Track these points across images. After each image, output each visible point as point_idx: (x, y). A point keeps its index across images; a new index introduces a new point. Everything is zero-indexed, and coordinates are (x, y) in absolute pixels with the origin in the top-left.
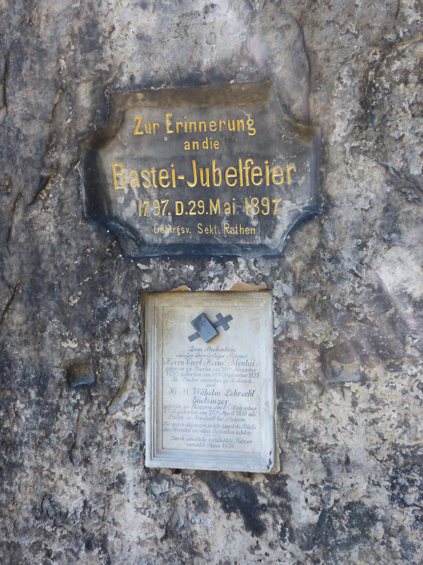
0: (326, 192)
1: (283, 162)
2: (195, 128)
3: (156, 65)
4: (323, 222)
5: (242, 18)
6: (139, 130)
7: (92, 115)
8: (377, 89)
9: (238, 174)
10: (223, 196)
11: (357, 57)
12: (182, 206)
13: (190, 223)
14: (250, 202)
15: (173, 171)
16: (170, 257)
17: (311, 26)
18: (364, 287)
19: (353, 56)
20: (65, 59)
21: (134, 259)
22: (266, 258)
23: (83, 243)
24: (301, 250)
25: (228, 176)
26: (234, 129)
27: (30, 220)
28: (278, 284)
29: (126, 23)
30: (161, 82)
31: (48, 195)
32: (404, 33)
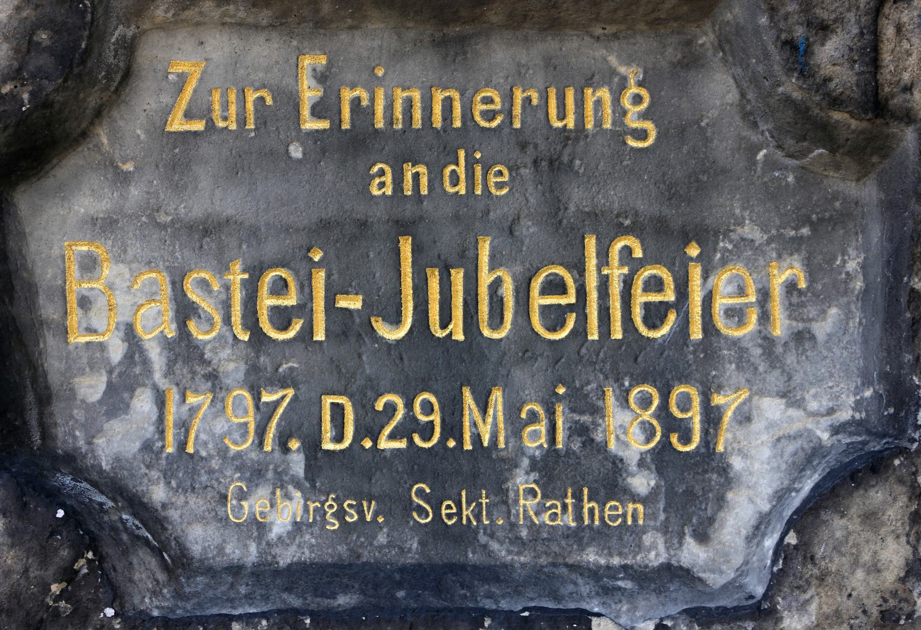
1: (759, 250)
2: (417, 114)
6: (189, 115)
7: (17, 50)
9: (582, 293)
13: (381, 483)
14: (624, 401)
15: (319, 279)
24: (841, 588)
25: (538, 301)
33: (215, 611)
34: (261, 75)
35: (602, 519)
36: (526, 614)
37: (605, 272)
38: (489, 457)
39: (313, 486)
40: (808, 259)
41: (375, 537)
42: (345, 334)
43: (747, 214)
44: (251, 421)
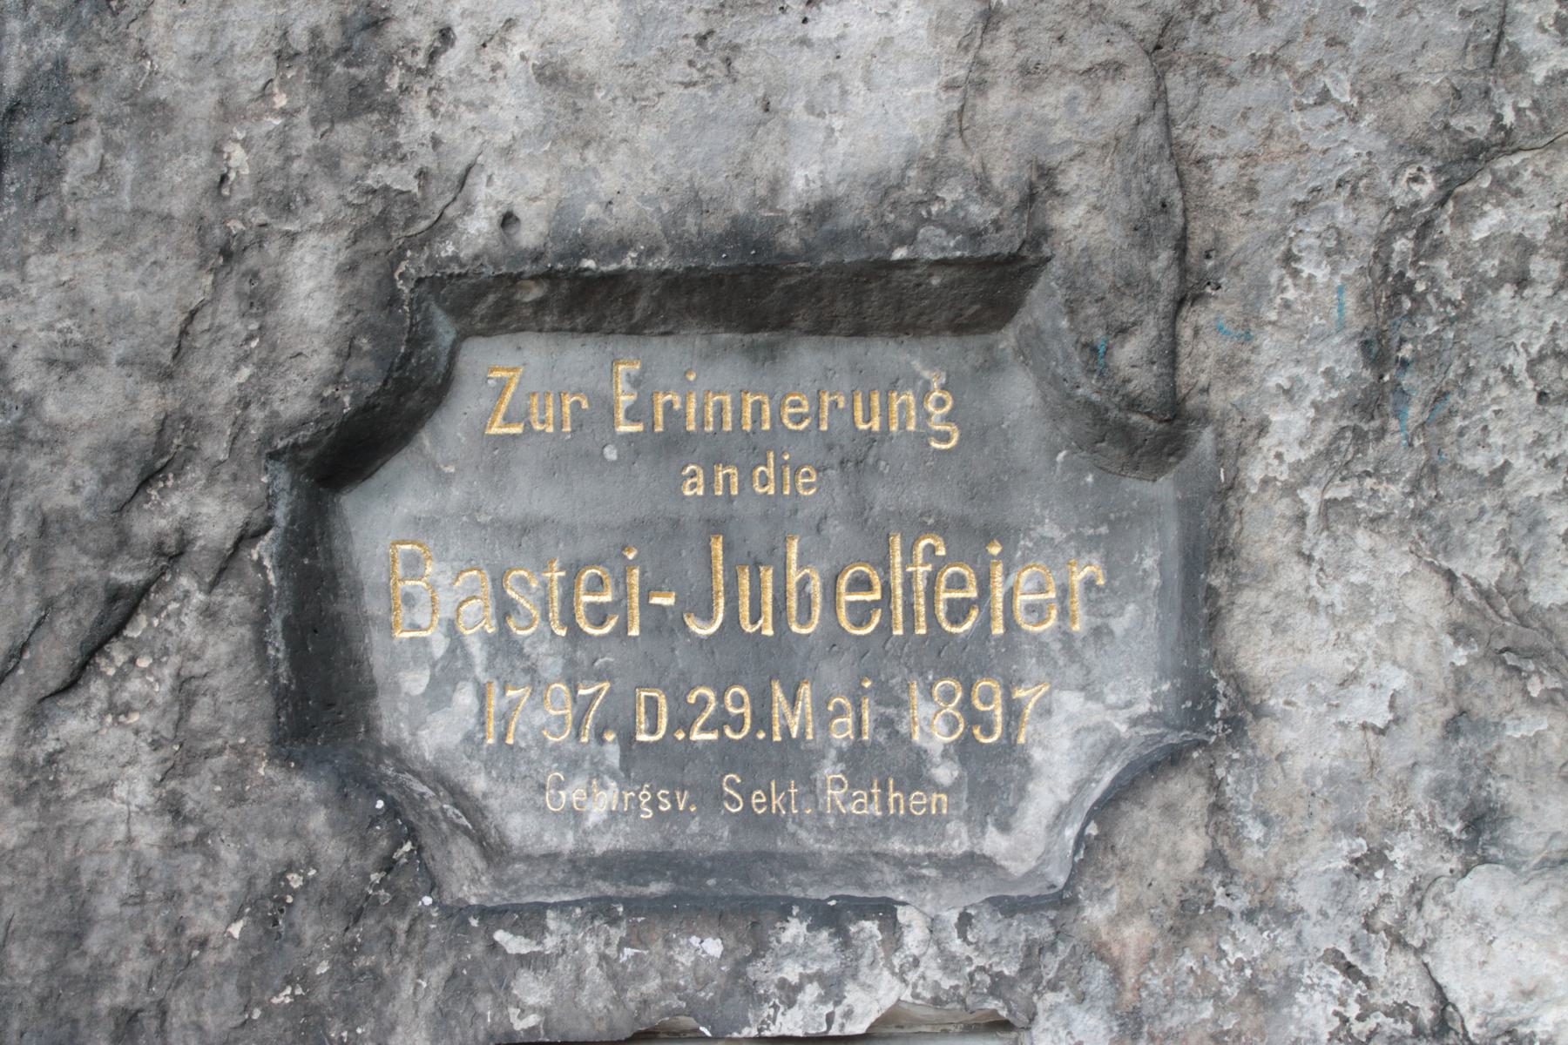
0: (1229, 662)
2: (728, 417)
3: (608, 182)
4: (1220, 772)
5: (951, 31)
6: (508, 420)
8: (1418, 300)
9: (887, 589)
10: (826, 669)
11: (1354, 188)
12: (663, 710)
14: (928, 694)
15: (635, 577)
16: (626, 902)
17: (1193, 71)
18: (1381, 1018)
19: (1340, 184)
20: (246, 144)
21: (483, 912)
22: (1007, 907)
23: (276, 851)
25: (846, 598)
26: (876, 425)
27: (51, 759)
28: (1052, 1009)
29: (496, 24)
30: (623, 246)
31: (133, 661)
32: (1519, 111)
33: (530, 899)
34: (577, 379)
35: (907, 808)
36: (833, 903)
37: (910, 569)
38: (798, 748)
39: (628, 776)
40: (1107, 556)
41: (687, 826)
42: (658, 628)
43: (1046, 512)
44: (569, 713)
